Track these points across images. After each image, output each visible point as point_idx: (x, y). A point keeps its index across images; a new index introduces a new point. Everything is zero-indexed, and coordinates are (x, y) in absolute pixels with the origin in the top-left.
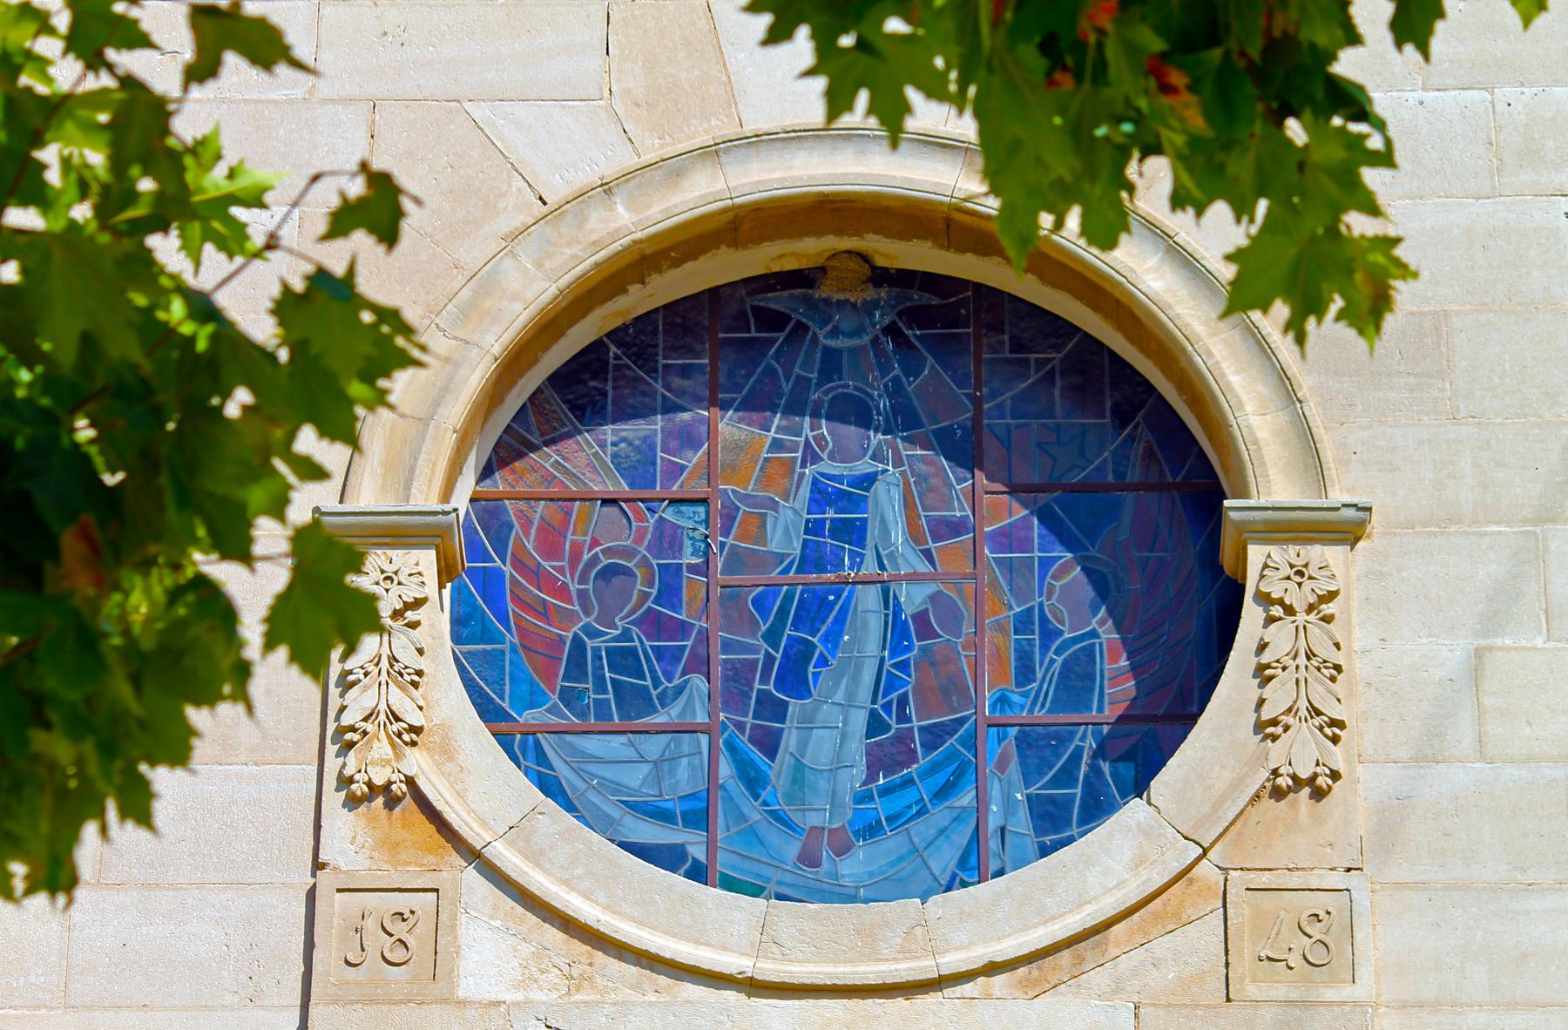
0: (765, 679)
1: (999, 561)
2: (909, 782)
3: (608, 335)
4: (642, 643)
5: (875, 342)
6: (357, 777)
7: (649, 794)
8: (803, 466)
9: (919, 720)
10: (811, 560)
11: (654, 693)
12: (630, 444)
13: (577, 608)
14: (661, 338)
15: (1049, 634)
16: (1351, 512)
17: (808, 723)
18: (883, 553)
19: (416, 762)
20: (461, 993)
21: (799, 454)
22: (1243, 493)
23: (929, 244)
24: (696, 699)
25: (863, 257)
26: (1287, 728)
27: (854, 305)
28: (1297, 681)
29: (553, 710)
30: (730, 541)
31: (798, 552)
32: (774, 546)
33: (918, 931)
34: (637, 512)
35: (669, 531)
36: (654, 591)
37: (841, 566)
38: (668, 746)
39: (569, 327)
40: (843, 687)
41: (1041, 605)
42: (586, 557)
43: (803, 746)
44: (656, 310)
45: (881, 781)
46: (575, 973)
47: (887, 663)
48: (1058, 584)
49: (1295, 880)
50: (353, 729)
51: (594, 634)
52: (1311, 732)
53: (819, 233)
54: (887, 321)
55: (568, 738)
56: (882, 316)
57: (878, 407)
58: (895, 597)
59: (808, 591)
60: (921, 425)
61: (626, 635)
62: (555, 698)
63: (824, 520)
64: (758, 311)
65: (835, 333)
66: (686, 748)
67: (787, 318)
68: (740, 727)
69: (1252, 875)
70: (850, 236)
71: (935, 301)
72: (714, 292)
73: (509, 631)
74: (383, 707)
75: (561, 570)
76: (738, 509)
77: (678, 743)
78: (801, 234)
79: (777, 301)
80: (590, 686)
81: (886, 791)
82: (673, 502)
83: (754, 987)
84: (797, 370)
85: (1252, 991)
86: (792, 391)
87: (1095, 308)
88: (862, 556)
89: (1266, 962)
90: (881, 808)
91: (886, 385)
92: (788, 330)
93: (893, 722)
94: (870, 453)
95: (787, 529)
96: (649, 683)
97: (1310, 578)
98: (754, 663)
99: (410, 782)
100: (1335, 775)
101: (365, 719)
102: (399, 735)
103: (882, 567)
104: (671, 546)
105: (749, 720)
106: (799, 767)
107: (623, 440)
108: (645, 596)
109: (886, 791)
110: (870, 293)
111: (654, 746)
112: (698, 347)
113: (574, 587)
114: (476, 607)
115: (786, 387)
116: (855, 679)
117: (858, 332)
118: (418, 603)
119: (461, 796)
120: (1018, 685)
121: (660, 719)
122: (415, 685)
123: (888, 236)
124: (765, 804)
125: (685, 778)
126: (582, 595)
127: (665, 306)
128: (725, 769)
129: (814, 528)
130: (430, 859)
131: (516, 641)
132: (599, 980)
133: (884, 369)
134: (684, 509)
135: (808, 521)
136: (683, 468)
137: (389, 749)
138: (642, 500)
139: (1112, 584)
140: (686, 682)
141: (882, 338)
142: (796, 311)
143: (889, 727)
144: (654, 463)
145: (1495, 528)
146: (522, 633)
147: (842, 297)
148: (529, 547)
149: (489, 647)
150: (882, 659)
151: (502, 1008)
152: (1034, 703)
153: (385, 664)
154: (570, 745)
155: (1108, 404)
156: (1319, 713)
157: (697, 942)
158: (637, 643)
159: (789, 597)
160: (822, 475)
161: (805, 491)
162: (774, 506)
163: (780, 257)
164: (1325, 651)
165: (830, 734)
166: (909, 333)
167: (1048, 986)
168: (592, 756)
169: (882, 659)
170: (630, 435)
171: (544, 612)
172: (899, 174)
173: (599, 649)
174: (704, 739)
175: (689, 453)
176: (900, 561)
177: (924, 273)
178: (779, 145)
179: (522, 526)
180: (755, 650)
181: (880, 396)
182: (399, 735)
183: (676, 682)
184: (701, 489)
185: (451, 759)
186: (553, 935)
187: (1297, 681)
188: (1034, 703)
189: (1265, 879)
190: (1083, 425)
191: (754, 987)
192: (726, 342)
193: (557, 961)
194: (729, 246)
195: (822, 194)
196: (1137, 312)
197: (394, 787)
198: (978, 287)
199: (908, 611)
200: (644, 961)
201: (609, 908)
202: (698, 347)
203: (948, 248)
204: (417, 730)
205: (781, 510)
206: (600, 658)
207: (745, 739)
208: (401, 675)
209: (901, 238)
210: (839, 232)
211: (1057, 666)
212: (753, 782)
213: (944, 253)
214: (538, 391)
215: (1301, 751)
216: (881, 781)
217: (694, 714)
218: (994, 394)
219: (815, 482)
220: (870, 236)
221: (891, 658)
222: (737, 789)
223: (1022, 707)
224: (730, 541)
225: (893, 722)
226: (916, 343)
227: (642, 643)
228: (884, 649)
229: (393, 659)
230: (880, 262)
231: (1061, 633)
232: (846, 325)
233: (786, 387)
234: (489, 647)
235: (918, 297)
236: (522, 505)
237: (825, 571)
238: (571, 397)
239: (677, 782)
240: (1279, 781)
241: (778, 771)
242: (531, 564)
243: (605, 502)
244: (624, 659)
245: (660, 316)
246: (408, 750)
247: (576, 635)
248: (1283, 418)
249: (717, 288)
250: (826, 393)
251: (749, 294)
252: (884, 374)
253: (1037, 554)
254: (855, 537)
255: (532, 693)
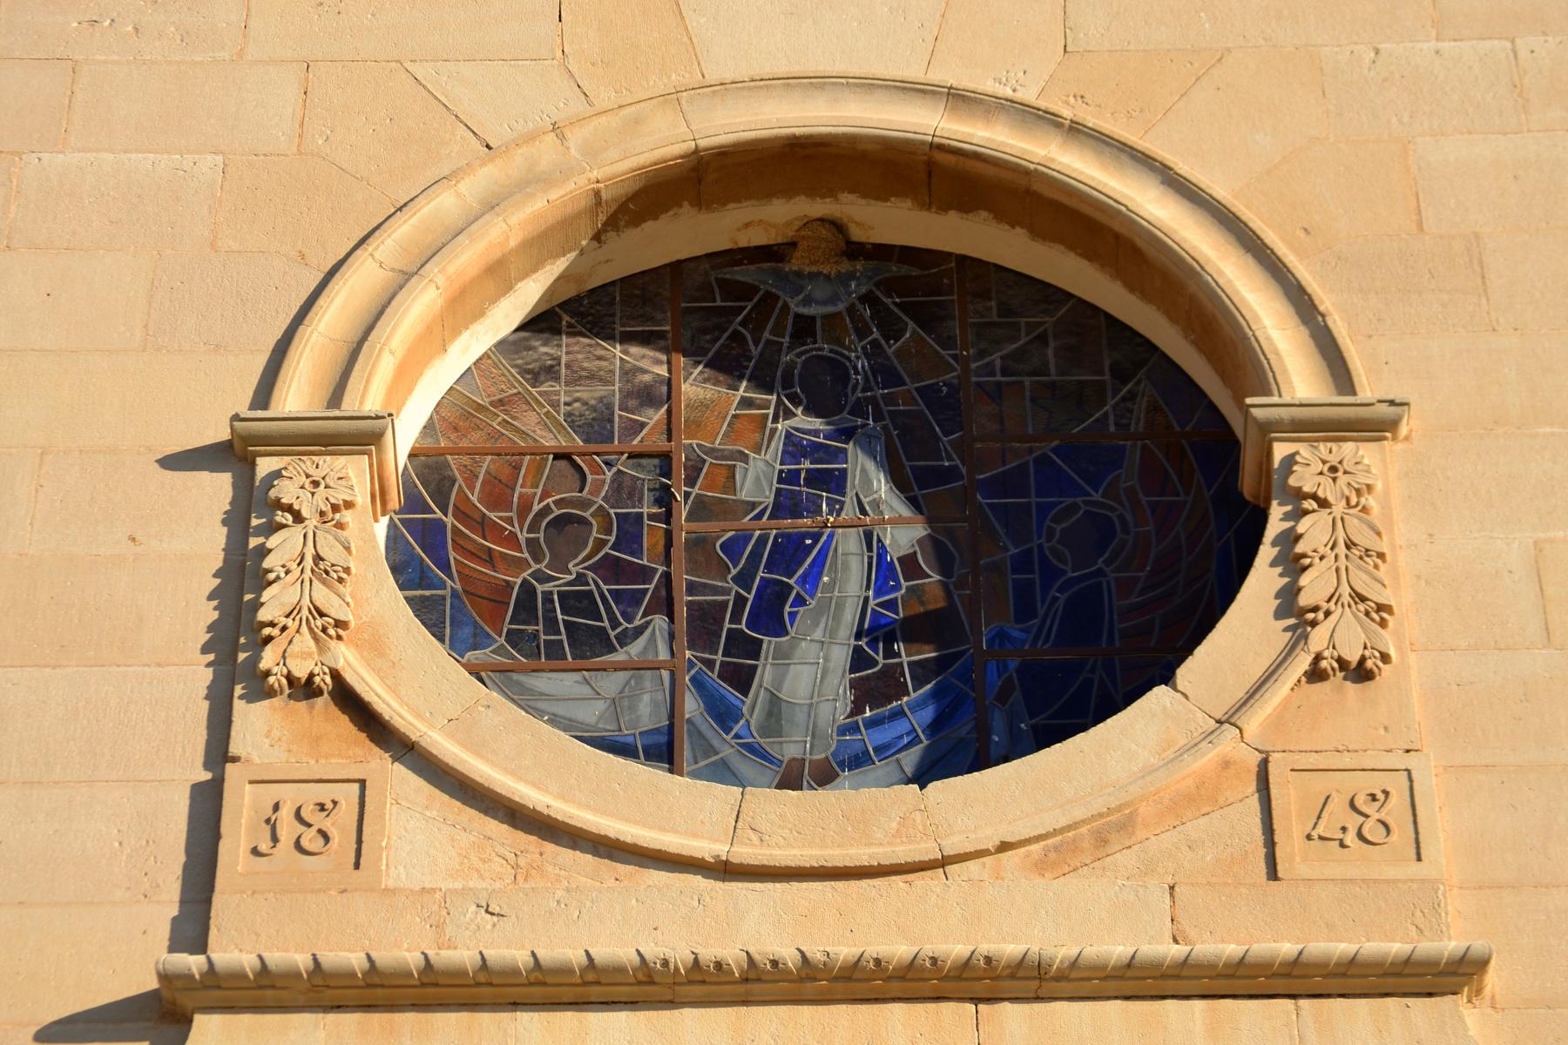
0: (736, 618)
1: (992, 507)
2: (899, 714)
3: (561, 305)
4: (598, 586)
5: (851, 309)
6: (275, 670)
7: (607, 729)
8: (776, 419)
9: (909, 664)
10: (785, 505)
11: (612, 634)
12: (585, 403)
13: (526, 555)
14: (618, 308)
15: (1050, 574)
16: (1384, 408)
17: (783, 655)
18: (865, 501)
19: (348, 659)
20: (388, 882)
21: (771, 411)
22: (1267, 392)
23: (909, 203)
24: (654, 638)
25: (837, 226)
26: (1328, 614)
27: (828, 277)
28: (1337, 570)
29: (500, 651)
30: (696, 491)
31: (772, 499)
32: (745, 493)
33: (918, 817)
34: (593, 464)
35: (627, 482)
36: (613, 539)
37: (819, 512)
38: (628, 683)
39: (521, 279)
40: (822, 625)
41: (1040, 546)
42: (536, 508)
43: (779, 681)
44: (613, 283)
45: (868, 714)
46: (522, 862)
47: (872, 603)
48: (1058, 528)
49: (1347, 761)
50: (272, 624)
51: (541, 578)
52: (1356, 617)
53: (788, 193)
54: (863, 290)
55: (515, 676)
56: (858, 286)
57: (855, 368)
58: (879, 540)
59: (782, 535)
60: (904, 384)
61: (581, 579)
62: (502, 640)
63: (799, 471)
64: (723, 283)
65: (807, 301)
66: (648, 684)
67: (756, 289)
68: (710, 664)
69: (1297, 756)
70: (823, 197)
71: (915, 272)
72: (676, 267)
73: (450, 577)
74: (306, 602)
75: (509, 521)
76: (704, 461)
77: (639, 680)
78: (769, 195)
79: (744, 274)
80: (541, 627)
81: (872, 724)
82: (632, 456)
83: (726, 871)
84: (766, 335)
85: (1303, 870)
86: (761, 355)
87: (1090, 255)
88: (842, 503)
89: (1317, 843)
90: (870, 739)
91: (864, 348)
92: (756, 299)
93: (880, 658)
94: (848, 408)
95: (758, 479)
96: (606, 624)
97: (1345, 472)
98: (724, 604)
99: (336, 675)
100: (1385, 658)
101: (287, 616)
102: (324, 630)
103: (863, 511)
104: (631, 495)
105: (719, 658)
106: (774, 701)
107: (577, 400)
108: (603, 543)
109: (872, 724)
110: (845, 266)
111: (611, 683)
112: (659, 316)
113: (523, 536)
114: (414, 556)
115: (755, 351)
116: (837, 618)
117: (834, 299)
118: (349, 505)
119: (394, 690)
120: (1017, 621)
121: (619, 656)
122: (341, 580)
123: (865, 196)
124: (737, 736)
125: (647, 713)
126: (532, 544)
127: (622, 280)
128: (691, 705)
129: (789, 478)
130: (359, 751)
131: (458, 587)
132: (550, 869)
133: (862, 333)
134: (644, 461)
135: (781, 472)
136: (643, 425)
137: (312, 643)
138: (598, 454)
139: (1118, 528)
140: (648, 623)
141: (860, 307)
142: (765, 283)
143: (877, 663)
144: (611, 421)
145: (1548, 430)
146: (464, 578)
147: (814, 269)
148: (474, 499)
149: (427, 593)
150: (866, 599)
151: (438, 895)
152: (1037, 637)
153: (309, 562)
154: (518, 683)
155: (1107, 363)
156: (1363, 599)
157: (662, 829)
158: (593, 587)
159: (762, 541)
160: (797, 430)
161: (778, 445)
162: (744, 458)
163: (747, 225)
164: (1364, 538)
165: (811, 669)
166: (888, 301)
167: (1066, 869)
168: (542, 694)
169: (866, 599)
170: (584, 395)
171: (489, 558)
172: (875, 116)
173: (551, 593)
174: (665, 674)
175: (650, 412)
176: (882, 507)
177: (902, 247)
178: (745, 93)
179: (465, 480)
180: (727, 592)
181: (858, 358)
182: (324, 630)
183: (637, 622)
184: (661, 444)
185: (381, 655)
186: (498, 829)
187: (1337, 570)
188: (1037, 637)
189: (1312, 761)
190: (1080, 382)
191: (726, 871)
192: (688, 311)
193: (502, 851)
194: (691, 205)
195: (795, 137)
196: (1138, 242)
197: (317, 679)
198: (963, 260)
199: (893, 555)
200: (602, 849)
201: (561, 797)
202: (659, 316)
203: (929, 209)
204: (339, 624)
205: (751, 462)
206: (552, 601)
207: (715, 676)
208: (327, 573)
209: (878, 198)
210: (812, 192)
211: (1061, 603)
212: (724, 716)
213: (925, 214)
214: (485, 356)
215: (1343, 635)
216: (868, 714)
217: (657, 654)
218: (982, 354)
219: (788, 435)
220: (845, 197)
221: (875, 597)
222: (707, 726)
223: (1023, 642)
224: (696, 491)
225: (880, 658)
226: (896, 310)
227: (598, 586)
228: (868, 588)
229: (318, 558)
230: (857, 235)
231: (1064, 572)
232: (818, 295)
233: (755, 351)
234: (427, 593)
235: (895, 269)
236: (466, 460)
237: (802, 517)
238: (519, 362)
239: (638, 718)
240: (1324, 664)
241: (753, 707)
242: (477, 516)
243: (557, 457)
244: (577, 601)
245: (618, 288)
246: (333, 643)
247: (525, 581)
248: (1304, 332)
249: (679, 262)
250: (798, 355)
251: (713, 268)
252: (861, 337)
253: (1034, 499)
254: (833, 485)
255: (475, 635)
